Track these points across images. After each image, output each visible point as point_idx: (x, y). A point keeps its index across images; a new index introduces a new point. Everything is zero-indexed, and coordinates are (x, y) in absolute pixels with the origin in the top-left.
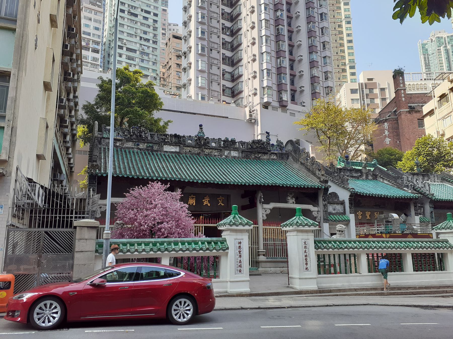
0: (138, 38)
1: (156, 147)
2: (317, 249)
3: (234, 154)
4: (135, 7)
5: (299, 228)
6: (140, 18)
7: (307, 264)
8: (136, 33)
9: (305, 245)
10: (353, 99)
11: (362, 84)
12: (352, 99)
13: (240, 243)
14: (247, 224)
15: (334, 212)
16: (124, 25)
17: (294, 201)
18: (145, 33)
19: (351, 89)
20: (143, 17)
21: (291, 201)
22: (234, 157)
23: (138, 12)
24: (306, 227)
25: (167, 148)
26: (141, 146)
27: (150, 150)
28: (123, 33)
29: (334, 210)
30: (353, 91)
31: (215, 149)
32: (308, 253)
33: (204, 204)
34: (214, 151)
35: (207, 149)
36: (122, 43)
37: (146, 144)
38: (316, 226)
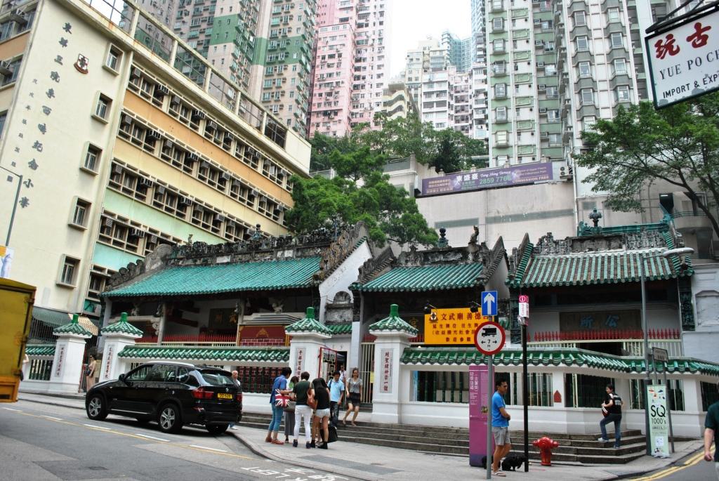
1: (209, 261)
3: (289, 253)
7: (107, 371)
13: (63, 349)
14: (137, 333)
15: (339, 320)
17: (280, 308)
21: (277, 309)
22: (287, 258)
25: (220, 260)
26: (198, 262)
27: (206, 264)
29: (341, 317)
31: (267, 252)
34: (266, 255)
35: (258, 253)
37: (202, 259)
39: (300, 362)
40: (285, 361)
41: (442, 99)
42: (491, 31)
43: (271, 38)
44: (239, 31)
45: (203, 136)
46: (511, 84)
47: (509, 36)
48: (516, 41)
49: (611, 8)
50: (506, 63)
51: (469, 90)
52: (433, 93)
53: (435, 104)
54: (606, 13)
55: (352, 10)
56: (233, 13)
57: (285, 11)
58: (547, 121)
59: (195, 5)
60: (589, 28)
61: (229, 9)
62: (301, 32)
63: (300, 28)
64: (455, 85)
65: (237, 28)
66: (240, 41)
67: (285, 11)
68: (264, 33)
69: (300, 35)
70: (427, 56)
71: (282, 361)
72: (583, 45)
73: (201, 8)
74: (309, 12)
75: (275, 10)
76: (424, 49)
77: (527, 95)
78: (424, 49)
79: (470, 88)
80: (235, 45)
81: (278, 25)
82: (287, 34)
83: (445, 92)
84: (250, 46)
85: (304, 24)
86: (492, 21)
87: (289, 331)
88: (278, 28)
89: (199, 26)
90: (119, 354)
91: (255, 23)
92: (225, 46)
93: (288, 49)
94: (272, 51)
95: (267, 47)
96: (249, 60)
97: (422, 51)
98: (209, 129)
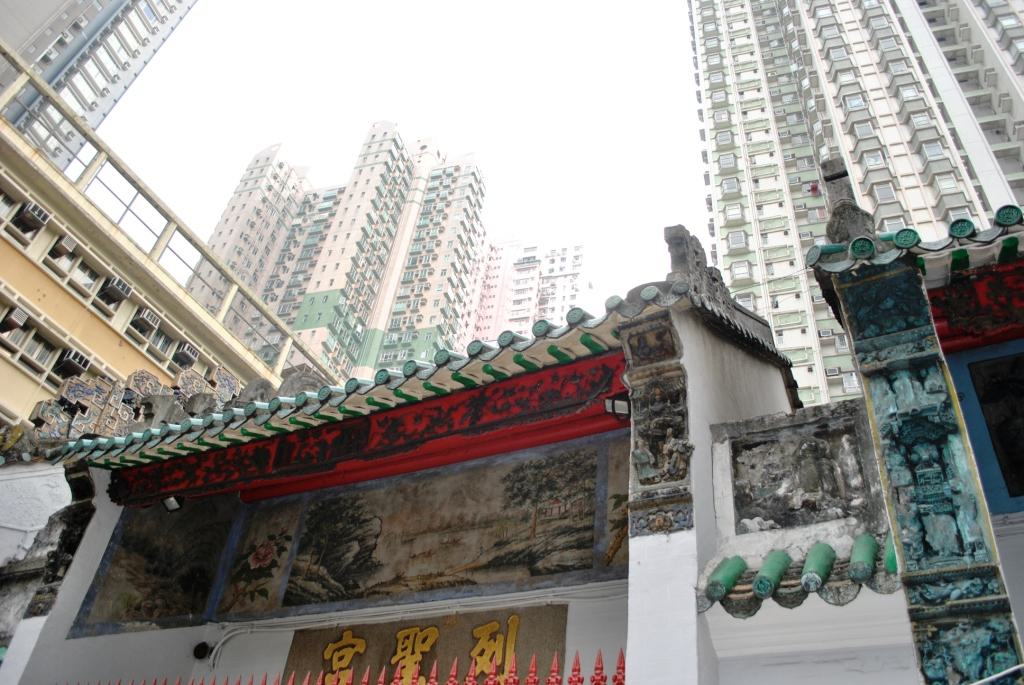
42: (726, 252)
43: (389, 330)
44: (340, 314)
45: (122, 333)
47: (758, 258)
48: (771, 264)
49: (938, 174)
50: (755, 297)
54: (931, 184)
55: (527, 321)
56: (334, 287)
57: (415, 293)
58: (844, 391)
59: (288, 287)
60: (905, 208)
61: (329, 282)
62: (436, 323)
63: (434, 317)
65: (337, 308)
66: (339, 327)
67: (415, 293)
68: (380, 321)
69: (434, 325)
73: (295, 291)
74: (452, 296)
75: (402, 292)
80: (329, 330)
81: (404, 313)
82: (415, 324)
84: (354, 337)
85: (443, 311)
86: (718, 161)
88: (402, 317)
89: (289, 314)
91: (368, 308)
92: (314, 332)
93: (414, 345)
94: (391, 347)
95: (382, 341)
96: (352, 359)
98: (139, 325)
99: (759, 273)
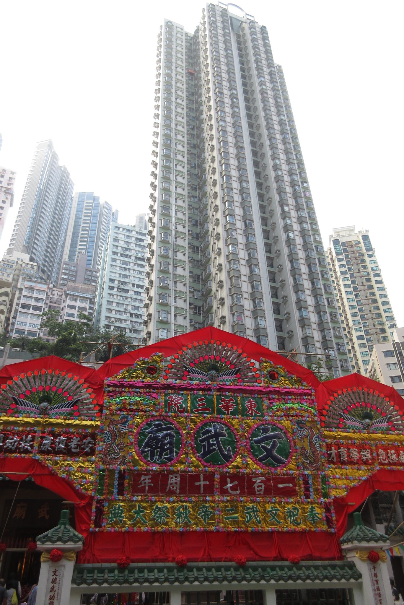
0: (129, 315)
2: (79, 584)
4: (126, 283)
5: (44, 546)
6: (131, 293)
8: (125, 309)
9: (54, 577)
10: (389, 364)
11: (397, 343)
12: (387, 364)
16: (112, 302)
18: (137, 308)
19: (384, 352)
20: (135, 292)
23: (129, 287)
24: (58, 543)
28: (112, 311)
30: (388, 354)
32: (56, 593)
33: (39, 517)
36: (109, 322)
38: (78, 541)
39: (377, 581)
40: (356, 579)
41: (37, 304)
46: (171, 313)
51: (62, 303)
52: (31, 297)
53: (31, 308)
64: (51, 296)
70: (20, 266)
71: (352, 580)
72: (238, 299)
76: (18, 259)
77: (183, 324)
78: (18, 259)
79: (64, 302)
83: (43, 300)
87: (360, 541)
90: (73, 581)
97: (16, 260)
99: (171, 285)
